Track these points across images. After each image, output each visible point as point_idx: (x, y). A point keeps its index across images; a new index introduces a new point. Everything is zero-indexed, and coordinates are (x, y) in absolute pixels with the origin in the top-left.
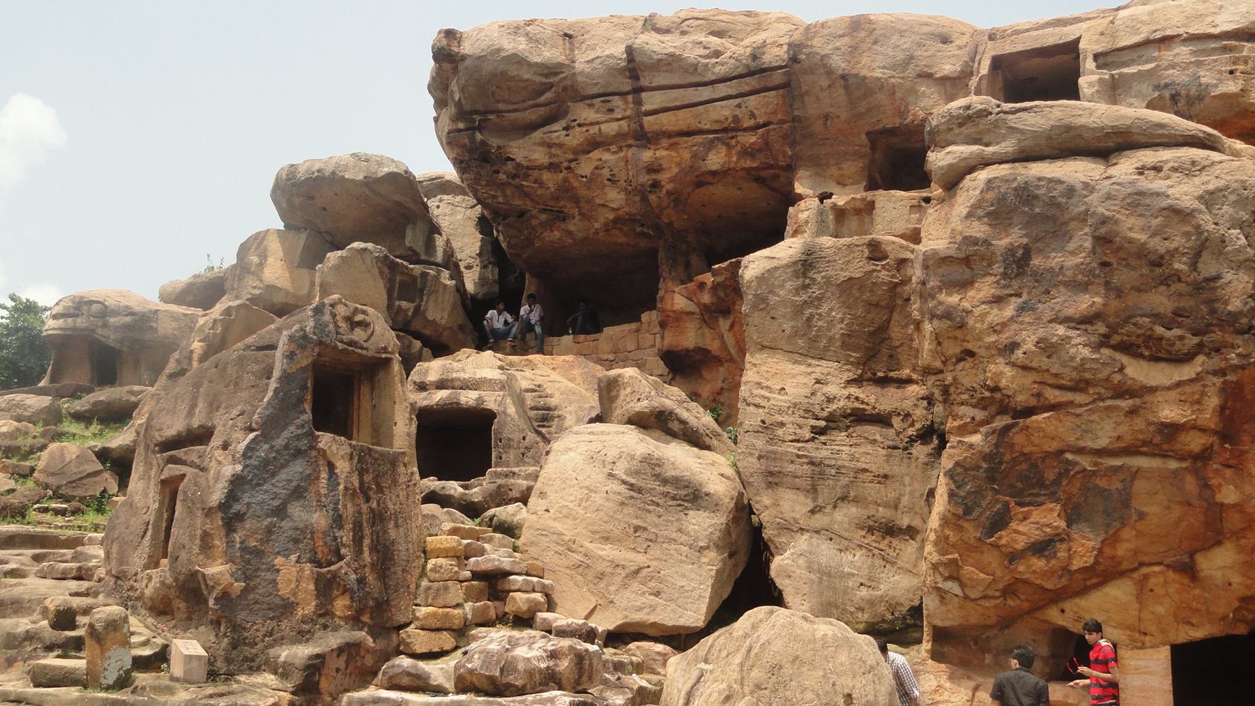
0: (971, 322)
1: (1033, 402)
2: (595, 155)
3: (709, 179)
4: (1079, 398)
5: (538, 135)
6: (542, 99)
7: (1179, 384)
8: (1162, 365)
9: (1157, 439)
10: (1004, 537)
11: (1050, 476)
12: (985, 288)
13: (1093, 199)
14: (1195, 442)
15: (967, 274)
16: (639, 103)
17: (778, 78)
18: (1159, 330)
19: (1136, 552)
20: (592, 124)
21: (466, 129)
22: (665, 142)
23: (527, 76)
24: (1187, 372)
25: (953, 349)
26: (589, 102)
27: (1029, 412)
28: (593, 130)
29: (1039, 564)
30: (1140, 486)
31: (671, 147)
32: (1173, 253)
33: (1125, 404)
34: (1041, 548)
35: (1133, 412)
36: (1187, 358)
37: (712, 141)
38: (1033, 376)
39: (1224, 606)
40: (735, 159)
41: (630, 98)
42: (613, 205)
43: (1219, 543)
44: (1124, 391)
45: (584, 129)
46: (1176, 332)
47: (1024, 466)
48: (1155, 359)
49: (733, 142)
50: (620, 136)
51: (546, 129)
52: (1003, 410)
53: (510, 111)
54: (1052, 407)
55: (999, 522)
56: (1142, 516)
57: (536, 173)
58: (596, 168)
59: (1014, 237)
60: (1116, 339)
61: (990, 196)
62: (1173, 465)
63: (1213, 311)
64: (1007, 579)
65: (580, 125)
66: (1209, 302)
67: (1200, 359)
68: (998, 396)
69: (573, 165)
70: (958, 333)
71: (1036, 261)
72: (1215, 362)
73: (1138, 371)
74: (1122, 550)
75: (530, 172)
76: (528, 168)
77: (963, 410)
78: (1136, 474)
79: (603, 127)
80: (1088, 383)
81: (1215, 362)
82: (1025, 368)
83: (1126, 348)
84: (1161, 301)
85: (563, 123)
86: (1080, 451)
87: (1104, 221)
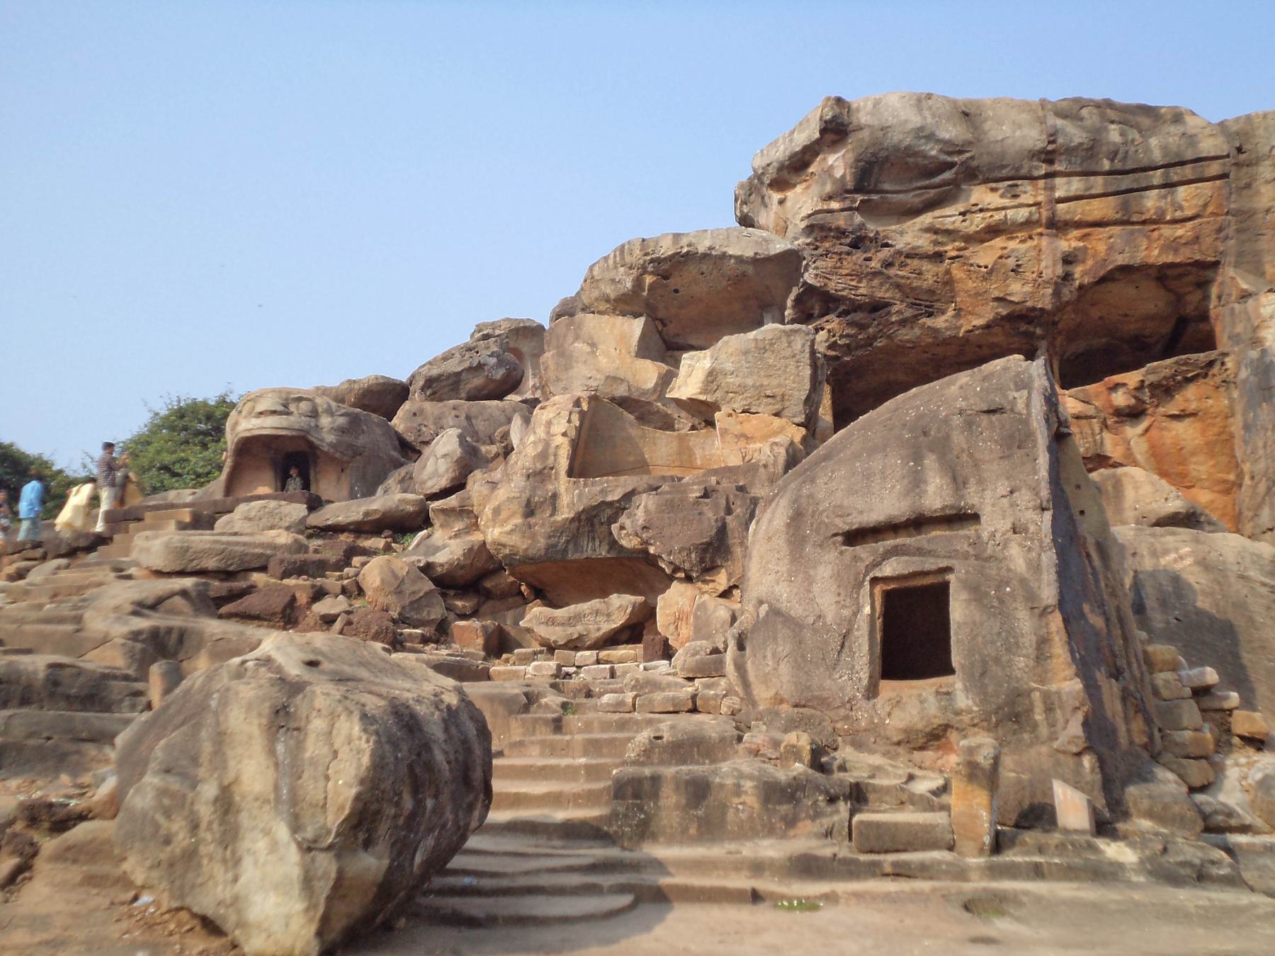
2: (998, 242)
3: (1117, 275)
5: (927, 219)
6: (938, 179)
16: (1052, 189)
17: (1214, 168)
20: (997, 209)
21: (842, 210)
22: (1076, 233)
23: (933, 153)
26: (994, 185)
28: (998, 216)
31: (1084, 237)
37: (1132, 233)
40: (1156, 252)
41: (1041, 183)
42: (1012, 299)
45: (989, 214)
49: (1156, 234)
50: (1028, 223)
51: (937, 213)
53: (892, 192)
57: (915, 263)
58: (1001, 257)
65: (981, 210)
69: (966, 253)
75: (909, 261)
76: (908, 256)
79: (1010, 213)
85: (961, 207)
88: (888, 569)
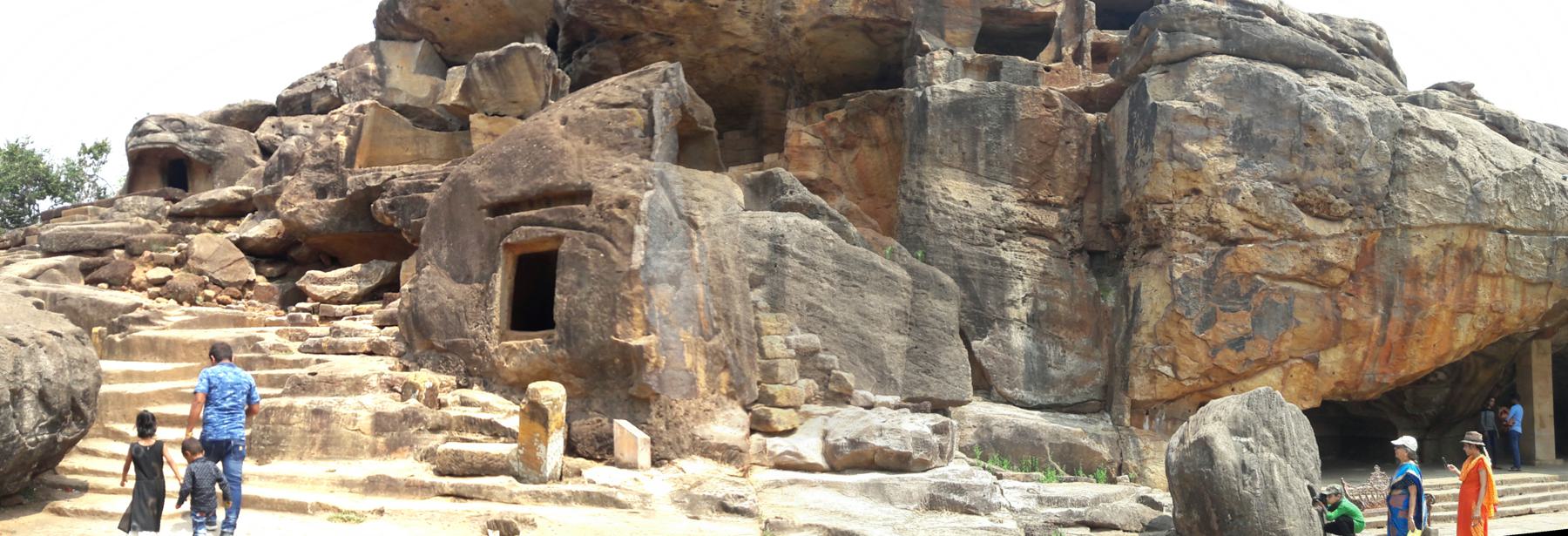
0: (1206, 167)
1: (1241, 235)
4: (1271, 237)
7: (1333, 236)
8: (1321, 222)
9: (1315, 272)
10: (1209, 335)
11: (1243, 290)
12: (1217, 146)
13: (1304, 97)
14: (1338, 276)
15: (1205, 132)
18: (1332, 197)
19: (1291, 349)
24: (1336, 229)
25: (1182, 186)
27: (1235, 242)
29: (1231, 353)
30: (1298, 302)
32: (1351, 147)
33: (1302, 245)
34: (1238, 344)
35: (1305, 251)
36: (1340, 219)
38: (1246, 216)
39: (1326, 388)
43: (1335, 346)
44: (1300, 236)
46: (1342, 201)
47: (1227, 282)
48: (1318, 217)
52: (1215, 237)
54: (1251, 241)
55: (1208, 322)
56: (1298, 323)
59: (1244, 111)
60: (1300, 198)
61: (1229, 77)
62: (1318, 291)
63: (1364, 191)
64: (1210, 365)
66: (1363, 185)
67: (1349, 222)
68: (1217, 227)
70: (1193, 176)
71: (1256, 131)
72: (1358, 226)
73: (1308, 223)
74: (1284, 347)
77: (1184, 234)
78: (1297, 294)
80: (1279, 225)
81: (1358, 226)
82: (1242, 210)
83: (1303, 206)
84: (1336, 178)
86: (1267, 275)
87: (1314, 115)
88: (520, 234)
